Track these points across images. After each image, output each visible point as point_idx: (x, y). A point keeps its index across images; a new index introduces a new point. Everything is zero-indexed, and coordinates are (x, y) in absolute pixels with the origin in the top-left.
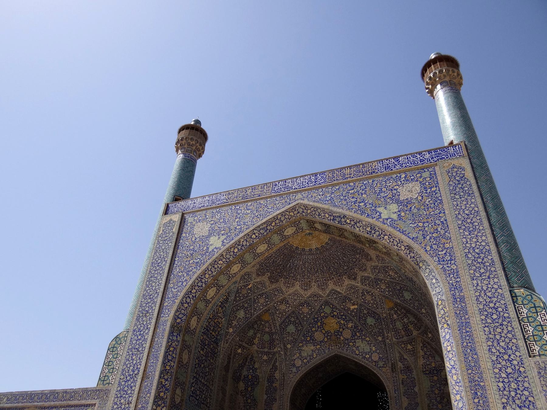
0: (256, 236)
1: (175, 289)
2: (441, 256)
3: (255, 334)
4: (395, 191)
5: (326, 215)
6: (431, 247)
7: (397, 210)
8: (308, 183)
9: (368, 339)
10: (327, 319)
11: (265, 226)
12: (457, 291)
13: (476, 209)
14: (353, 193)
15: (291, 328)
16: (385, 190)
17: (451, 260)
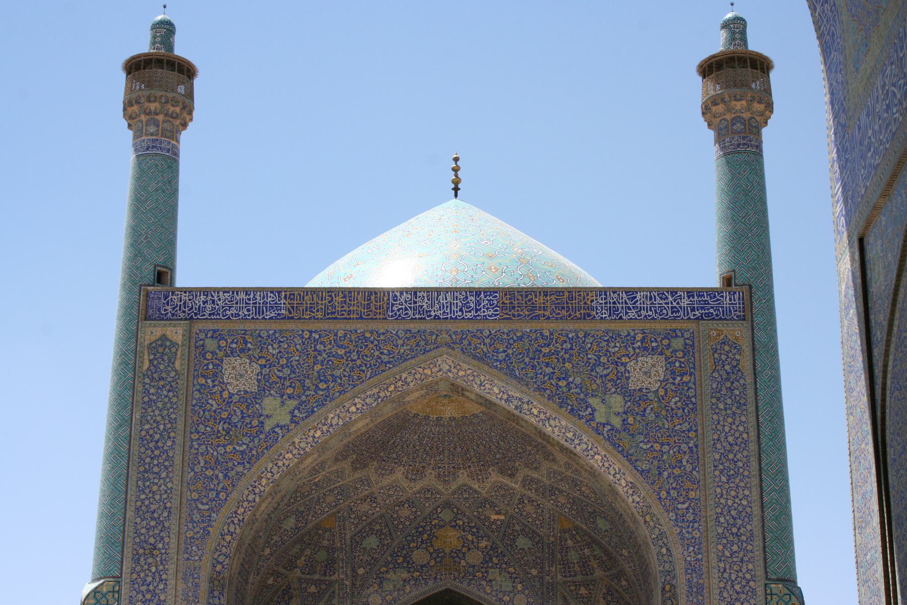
0: (358, 409)
1: (203, 504)
2: (680, 512)
3: (302, 550)
4: (622, 369)
5: (495, 389)
6: (668, 493)
7: (621, 410)
8: (461, 310)
9: (511, 570)
10: (442, 530)
11: (376, 390)
12: (694, 575)
13: (745, 436)
14: (550, 354)
15: (372, 542)
16: (606, 361)
17: (694, 521)
